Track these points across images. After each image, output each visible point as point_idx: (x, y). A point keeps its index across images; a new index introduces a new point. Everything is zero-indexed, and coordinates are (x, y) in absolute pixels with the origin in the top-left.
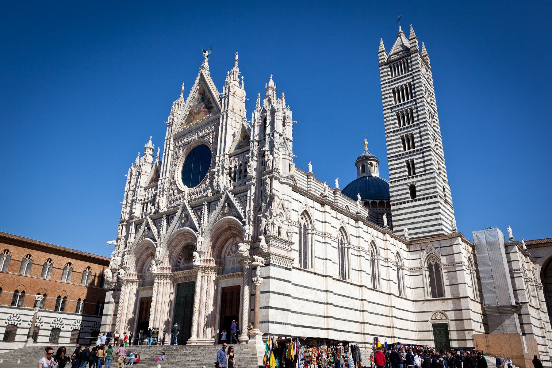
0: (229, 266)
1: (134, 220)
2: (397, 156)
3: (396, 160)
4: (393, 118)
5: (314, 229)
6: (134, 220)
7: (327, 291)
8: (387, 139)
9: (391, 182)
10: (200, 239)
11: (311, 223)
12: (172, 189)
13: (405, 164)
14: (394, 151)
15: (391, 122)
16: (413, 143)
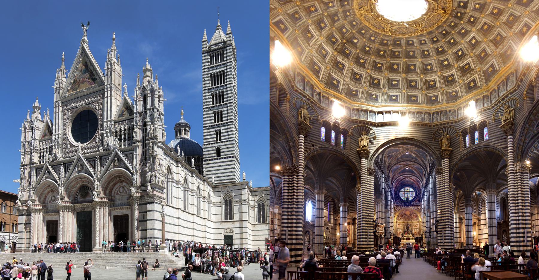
0: (118, 202)
1: (35, 165)
2: (209, 126)
3: (209, 129)
4: (210, 97)
5: (173, 179)
6: (35, 165)
7: (178, 218)
8: (204, 113)
9: (205, 145)
10: (96, 183)
11: (171, 175)
12: (65, 144)
13: (215, 133)
14: (208, 122)
15: (208, 100)
16: (222, 118)
